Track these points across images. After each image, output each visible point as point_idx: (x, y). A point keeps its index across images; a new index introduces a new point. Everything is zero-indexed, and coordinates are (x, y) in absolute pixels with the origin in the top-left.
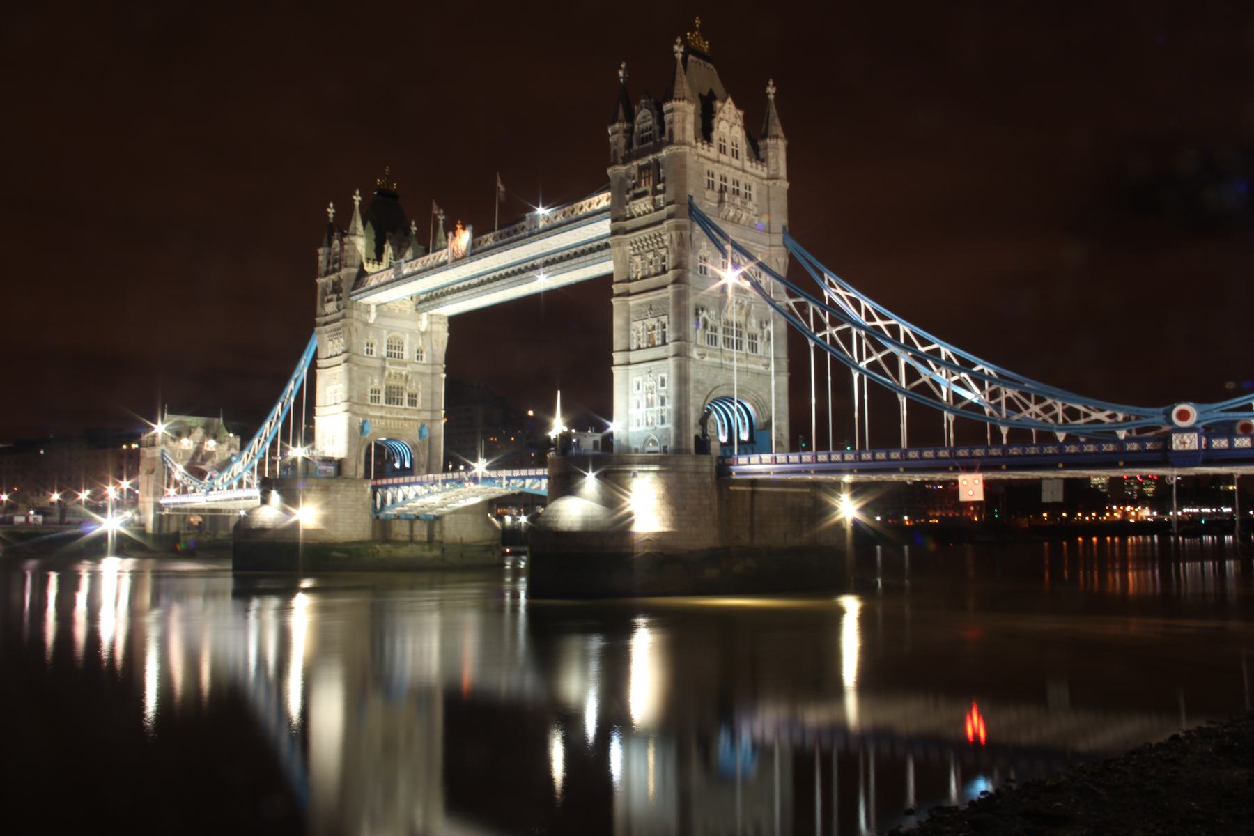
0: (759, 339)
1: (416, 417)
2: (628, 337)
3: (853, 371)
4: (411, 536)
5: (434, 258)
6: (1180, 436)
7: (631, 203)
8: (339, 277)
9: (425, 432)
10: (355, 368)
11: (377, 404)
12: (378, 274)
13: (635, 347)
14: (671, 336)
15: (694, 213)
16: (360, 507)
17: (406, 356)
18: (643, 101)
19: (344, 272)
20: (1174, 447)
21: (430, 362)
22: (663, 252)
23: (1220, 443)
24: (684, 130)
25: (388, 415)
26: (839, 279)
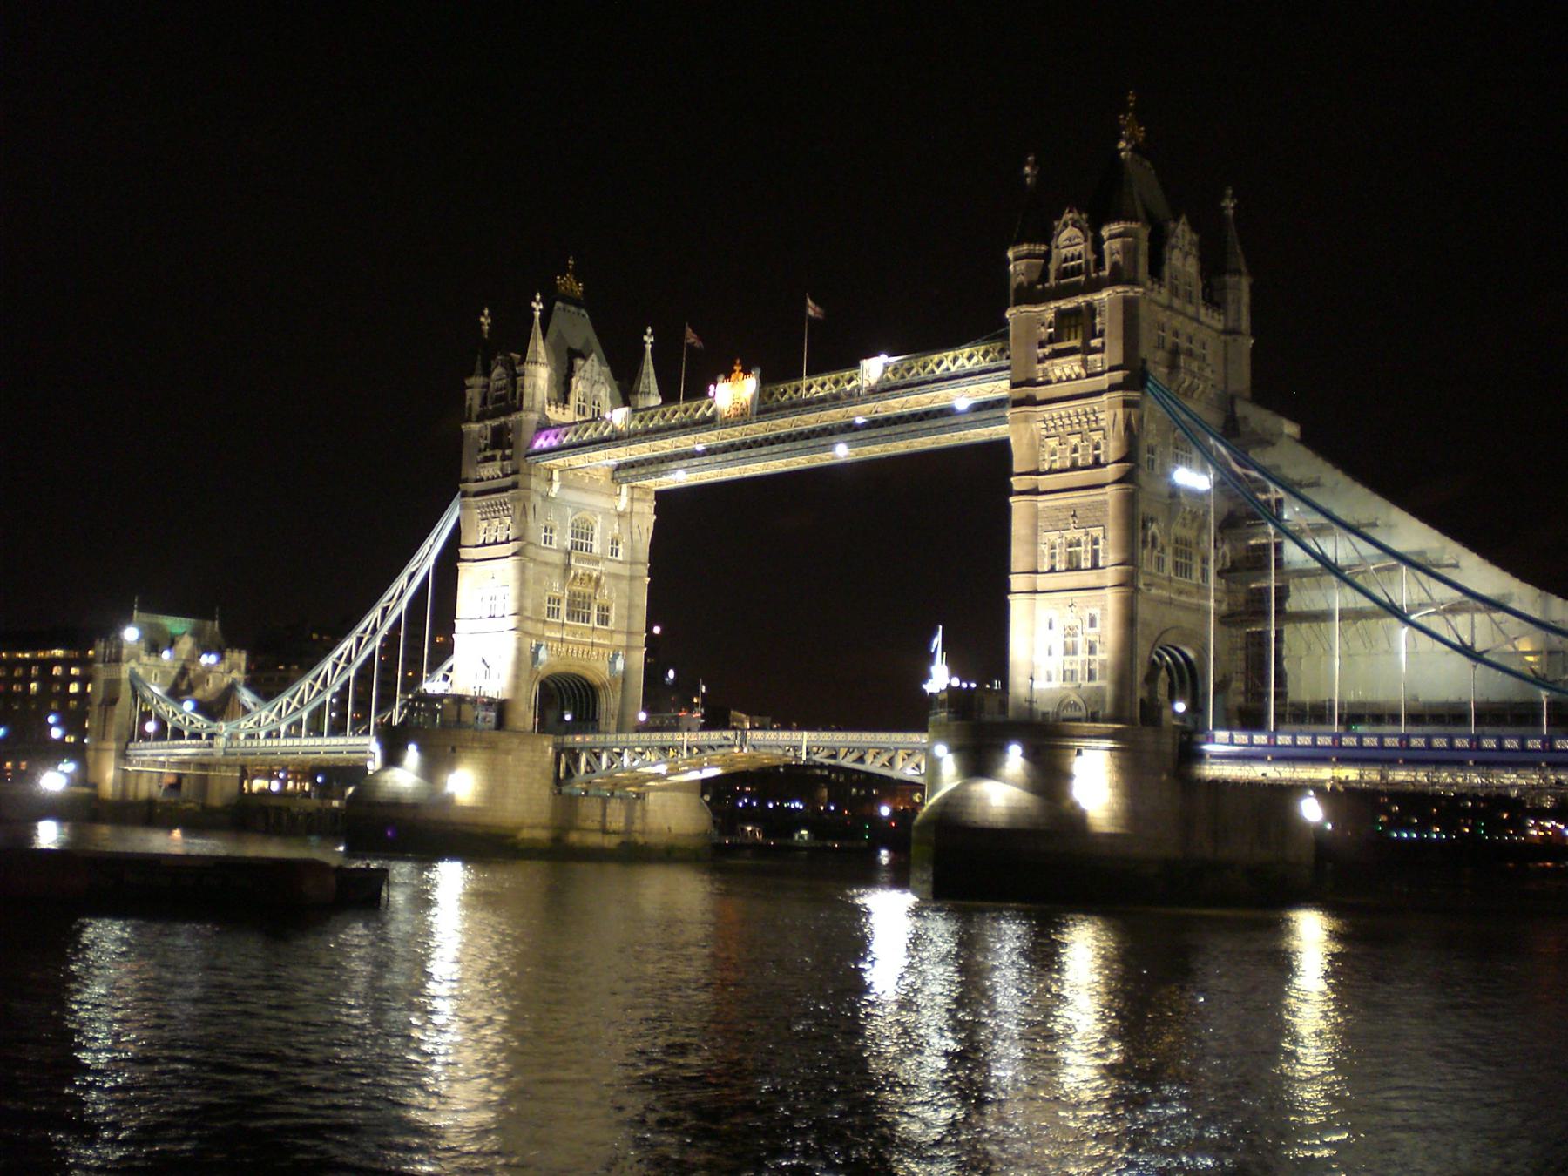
1: (606, 642)
2: (1035, 554)
5: (686, 411)
7: (1047, 364)
10: (532, 565)
11: (555, 620)
13: (1046, 569)
14: (1110, 555)
15: (1149, 385)
16: (538, 776)
17: (596, 549)
18: (1071, 215)
21: (629, 559)
22: (1097, 436)
25: (570, 638)
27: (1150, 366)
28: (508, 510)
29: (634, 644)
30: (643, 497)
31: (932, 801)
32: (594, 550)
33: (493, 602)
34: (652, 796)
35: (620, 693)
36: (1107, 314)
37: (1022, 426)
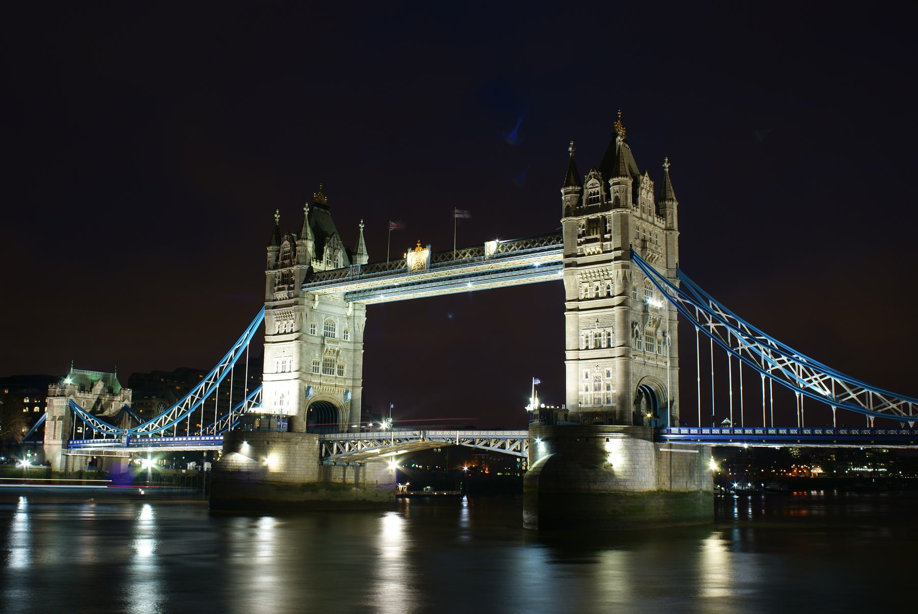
0: (662, 343)
1: (342, 384)
3: (762, 374)
4: (344, 479)
7: (583, 246)
8: (290, 270)
10: (305, 345)
13: (584, 348)
14: (617, 341)
15: (634, 257)
16: (311, 456)
18: (593, 173)
19: (294, 268)
21: (353, 341)
22: (608, 282)
25: (324, 382)
26: (720, 304)
27: (633, 248)
28: (291, 316)
31: (534, 465)
32: (336, 337)
33: (284, 364)
34: (368, 464)
35: (349, 411)
36: (613, 223)
37: (570, 277)
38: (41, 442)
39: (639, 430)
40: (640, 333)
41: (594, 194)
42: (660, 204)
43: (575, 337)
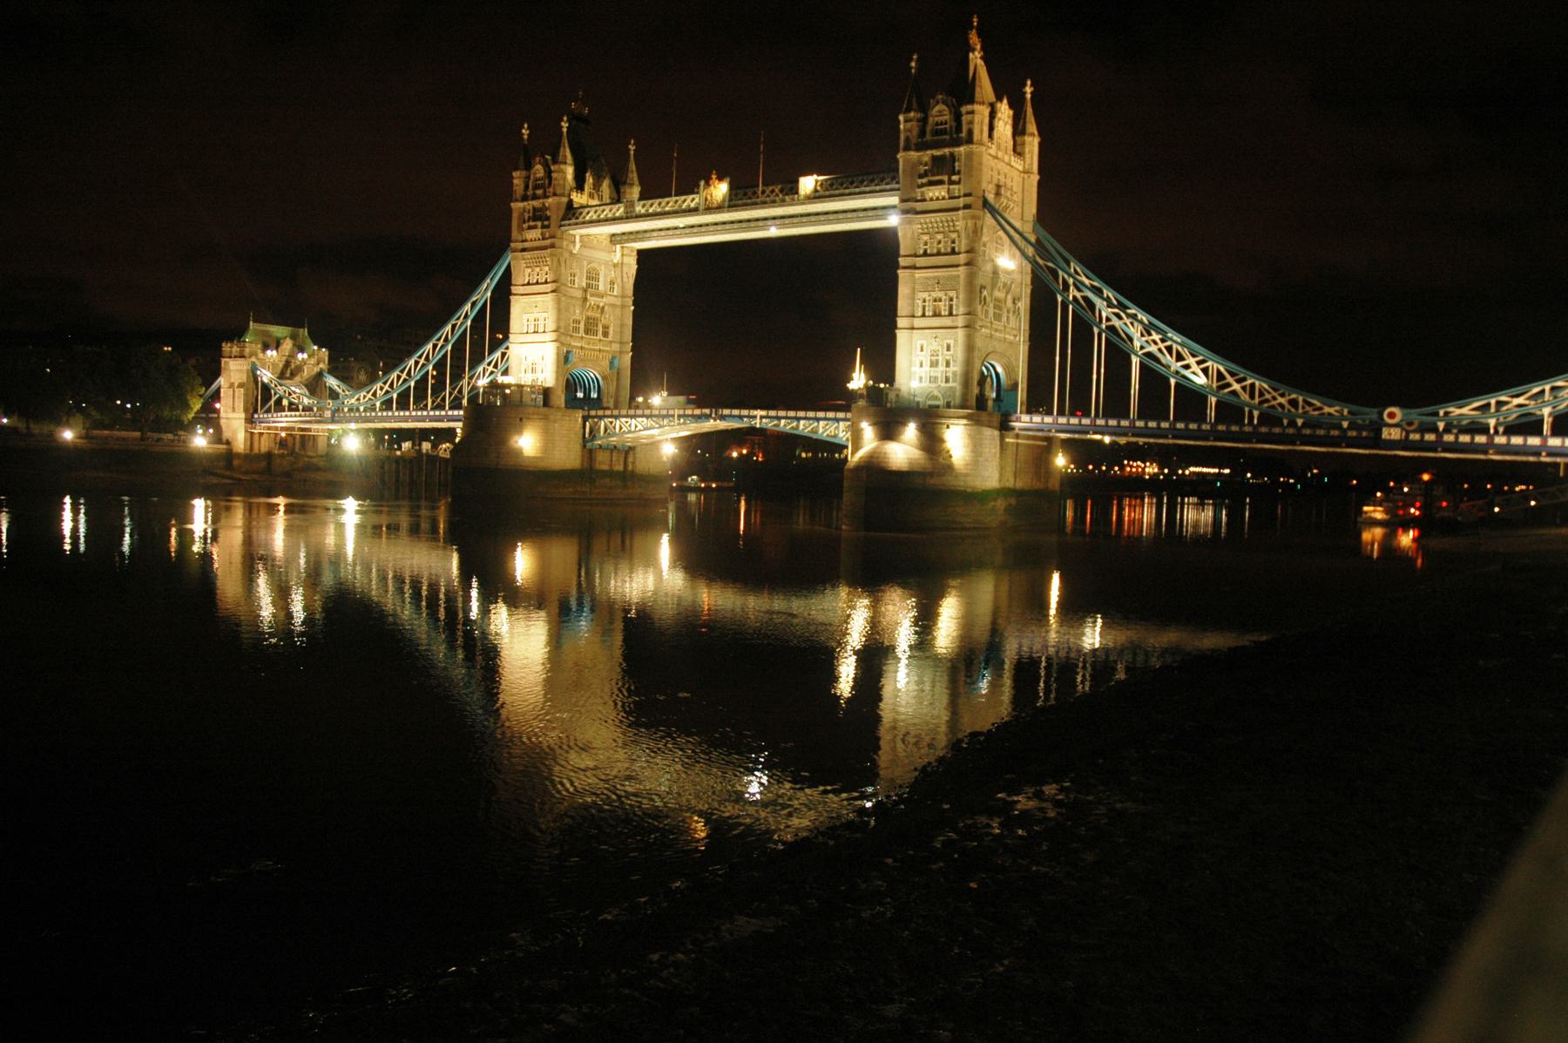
2: (913, 305)
5: (676, 201)
6: (1388, 429)
7: (923, 189)
8: (544, 204)
9: (616, 364)
10: (564, 299)
12: (598, 208)
13: (920, 314)
14: (962, 310)
16: (573, 436)
18: (940, 97)
20: (1383, 436)
22: (954, 236)
23: (1415, 437)
24: (982, 131)
27: (986, 194)
29: (624, 350)
30: (630, 253)
33: (536, 323)
37: (907, 226)
38: (216, 415)
39: (984, 416)
40: (988, 299)
41: (941, 124)
42: (1018, 139)
43: (910, 302)
